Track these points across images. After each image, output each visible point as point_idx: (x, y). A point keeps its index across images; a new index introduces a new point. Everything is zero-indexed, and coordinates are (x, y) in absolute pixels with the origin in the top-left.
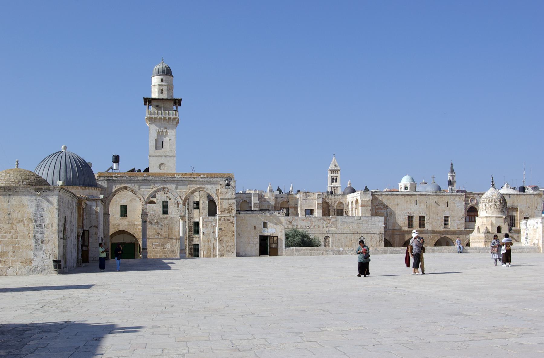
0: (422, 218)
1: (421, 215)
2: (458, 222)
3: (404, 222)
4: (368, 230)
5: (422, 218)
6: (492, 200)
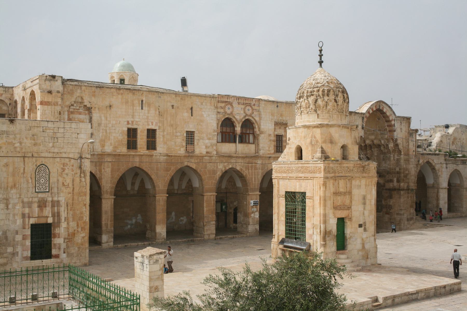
0: (151, 133)
1: (150, 127)
2: (207, 141)
3: (120, 138)
4: (56, 150)
5: (151, 133)
6: (329, 91)
